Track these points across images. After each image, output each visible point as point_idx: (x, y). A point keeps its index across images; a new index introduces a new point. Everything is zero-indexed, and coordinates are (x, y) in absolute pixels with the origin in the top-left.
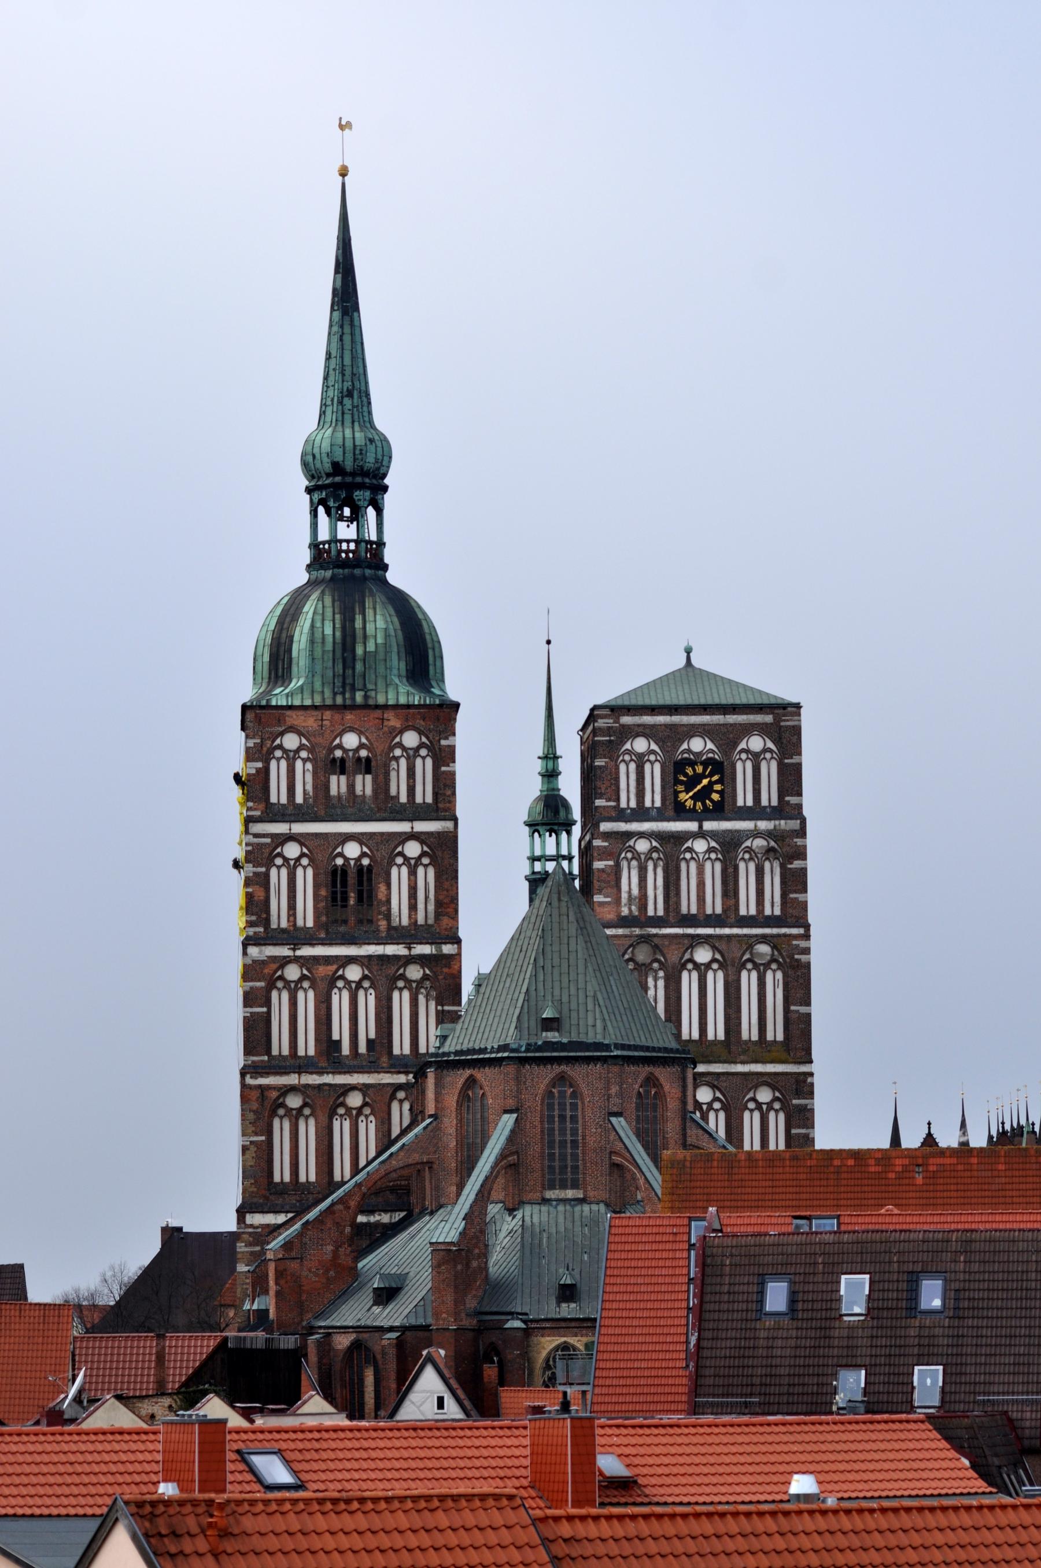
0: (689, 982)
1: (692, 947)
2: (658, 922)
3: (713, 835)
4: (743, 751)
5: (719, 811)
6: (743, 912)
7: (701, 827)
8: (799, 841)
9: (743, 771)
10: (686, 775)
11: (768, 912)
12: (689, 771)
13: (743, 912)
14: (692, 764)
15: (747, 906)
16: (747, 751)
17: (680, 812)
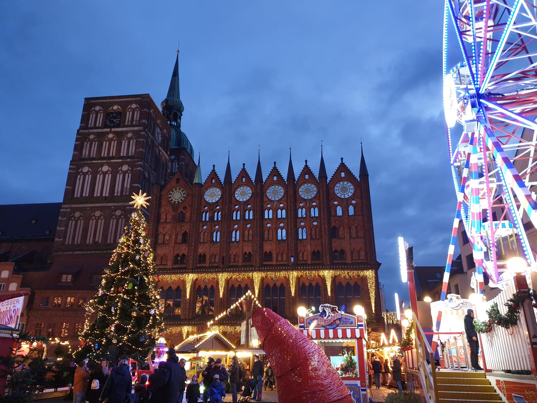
0: (99, 178)
1: (102, 166)
2: (94, 159)
3: (114, 133)
4: (129, 108)
5: (118, 126)
6: (122, 155)
7: (111, 130)
8: (143, 133)
9: (129, 115)
10: (110, 116)
11: (130, 154)
12: (111, 116)
13: (122, 155)
14: (112, 113)
15: (123, 153)
16: (131, 108)
17: (105, 126)
